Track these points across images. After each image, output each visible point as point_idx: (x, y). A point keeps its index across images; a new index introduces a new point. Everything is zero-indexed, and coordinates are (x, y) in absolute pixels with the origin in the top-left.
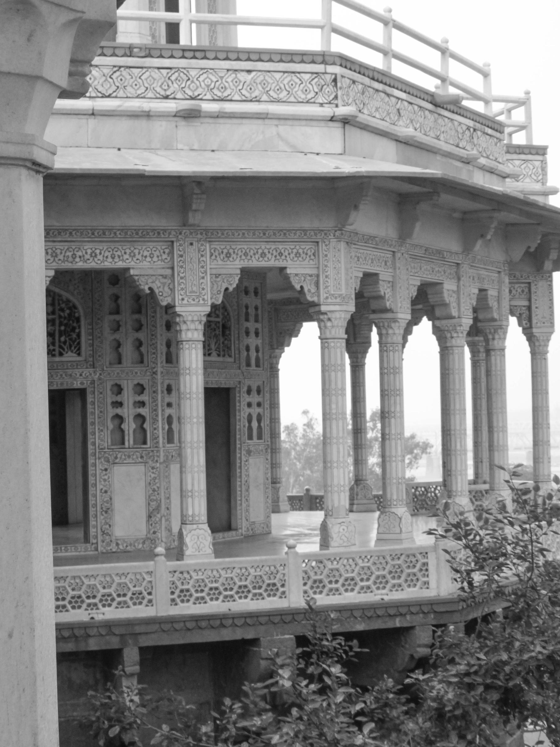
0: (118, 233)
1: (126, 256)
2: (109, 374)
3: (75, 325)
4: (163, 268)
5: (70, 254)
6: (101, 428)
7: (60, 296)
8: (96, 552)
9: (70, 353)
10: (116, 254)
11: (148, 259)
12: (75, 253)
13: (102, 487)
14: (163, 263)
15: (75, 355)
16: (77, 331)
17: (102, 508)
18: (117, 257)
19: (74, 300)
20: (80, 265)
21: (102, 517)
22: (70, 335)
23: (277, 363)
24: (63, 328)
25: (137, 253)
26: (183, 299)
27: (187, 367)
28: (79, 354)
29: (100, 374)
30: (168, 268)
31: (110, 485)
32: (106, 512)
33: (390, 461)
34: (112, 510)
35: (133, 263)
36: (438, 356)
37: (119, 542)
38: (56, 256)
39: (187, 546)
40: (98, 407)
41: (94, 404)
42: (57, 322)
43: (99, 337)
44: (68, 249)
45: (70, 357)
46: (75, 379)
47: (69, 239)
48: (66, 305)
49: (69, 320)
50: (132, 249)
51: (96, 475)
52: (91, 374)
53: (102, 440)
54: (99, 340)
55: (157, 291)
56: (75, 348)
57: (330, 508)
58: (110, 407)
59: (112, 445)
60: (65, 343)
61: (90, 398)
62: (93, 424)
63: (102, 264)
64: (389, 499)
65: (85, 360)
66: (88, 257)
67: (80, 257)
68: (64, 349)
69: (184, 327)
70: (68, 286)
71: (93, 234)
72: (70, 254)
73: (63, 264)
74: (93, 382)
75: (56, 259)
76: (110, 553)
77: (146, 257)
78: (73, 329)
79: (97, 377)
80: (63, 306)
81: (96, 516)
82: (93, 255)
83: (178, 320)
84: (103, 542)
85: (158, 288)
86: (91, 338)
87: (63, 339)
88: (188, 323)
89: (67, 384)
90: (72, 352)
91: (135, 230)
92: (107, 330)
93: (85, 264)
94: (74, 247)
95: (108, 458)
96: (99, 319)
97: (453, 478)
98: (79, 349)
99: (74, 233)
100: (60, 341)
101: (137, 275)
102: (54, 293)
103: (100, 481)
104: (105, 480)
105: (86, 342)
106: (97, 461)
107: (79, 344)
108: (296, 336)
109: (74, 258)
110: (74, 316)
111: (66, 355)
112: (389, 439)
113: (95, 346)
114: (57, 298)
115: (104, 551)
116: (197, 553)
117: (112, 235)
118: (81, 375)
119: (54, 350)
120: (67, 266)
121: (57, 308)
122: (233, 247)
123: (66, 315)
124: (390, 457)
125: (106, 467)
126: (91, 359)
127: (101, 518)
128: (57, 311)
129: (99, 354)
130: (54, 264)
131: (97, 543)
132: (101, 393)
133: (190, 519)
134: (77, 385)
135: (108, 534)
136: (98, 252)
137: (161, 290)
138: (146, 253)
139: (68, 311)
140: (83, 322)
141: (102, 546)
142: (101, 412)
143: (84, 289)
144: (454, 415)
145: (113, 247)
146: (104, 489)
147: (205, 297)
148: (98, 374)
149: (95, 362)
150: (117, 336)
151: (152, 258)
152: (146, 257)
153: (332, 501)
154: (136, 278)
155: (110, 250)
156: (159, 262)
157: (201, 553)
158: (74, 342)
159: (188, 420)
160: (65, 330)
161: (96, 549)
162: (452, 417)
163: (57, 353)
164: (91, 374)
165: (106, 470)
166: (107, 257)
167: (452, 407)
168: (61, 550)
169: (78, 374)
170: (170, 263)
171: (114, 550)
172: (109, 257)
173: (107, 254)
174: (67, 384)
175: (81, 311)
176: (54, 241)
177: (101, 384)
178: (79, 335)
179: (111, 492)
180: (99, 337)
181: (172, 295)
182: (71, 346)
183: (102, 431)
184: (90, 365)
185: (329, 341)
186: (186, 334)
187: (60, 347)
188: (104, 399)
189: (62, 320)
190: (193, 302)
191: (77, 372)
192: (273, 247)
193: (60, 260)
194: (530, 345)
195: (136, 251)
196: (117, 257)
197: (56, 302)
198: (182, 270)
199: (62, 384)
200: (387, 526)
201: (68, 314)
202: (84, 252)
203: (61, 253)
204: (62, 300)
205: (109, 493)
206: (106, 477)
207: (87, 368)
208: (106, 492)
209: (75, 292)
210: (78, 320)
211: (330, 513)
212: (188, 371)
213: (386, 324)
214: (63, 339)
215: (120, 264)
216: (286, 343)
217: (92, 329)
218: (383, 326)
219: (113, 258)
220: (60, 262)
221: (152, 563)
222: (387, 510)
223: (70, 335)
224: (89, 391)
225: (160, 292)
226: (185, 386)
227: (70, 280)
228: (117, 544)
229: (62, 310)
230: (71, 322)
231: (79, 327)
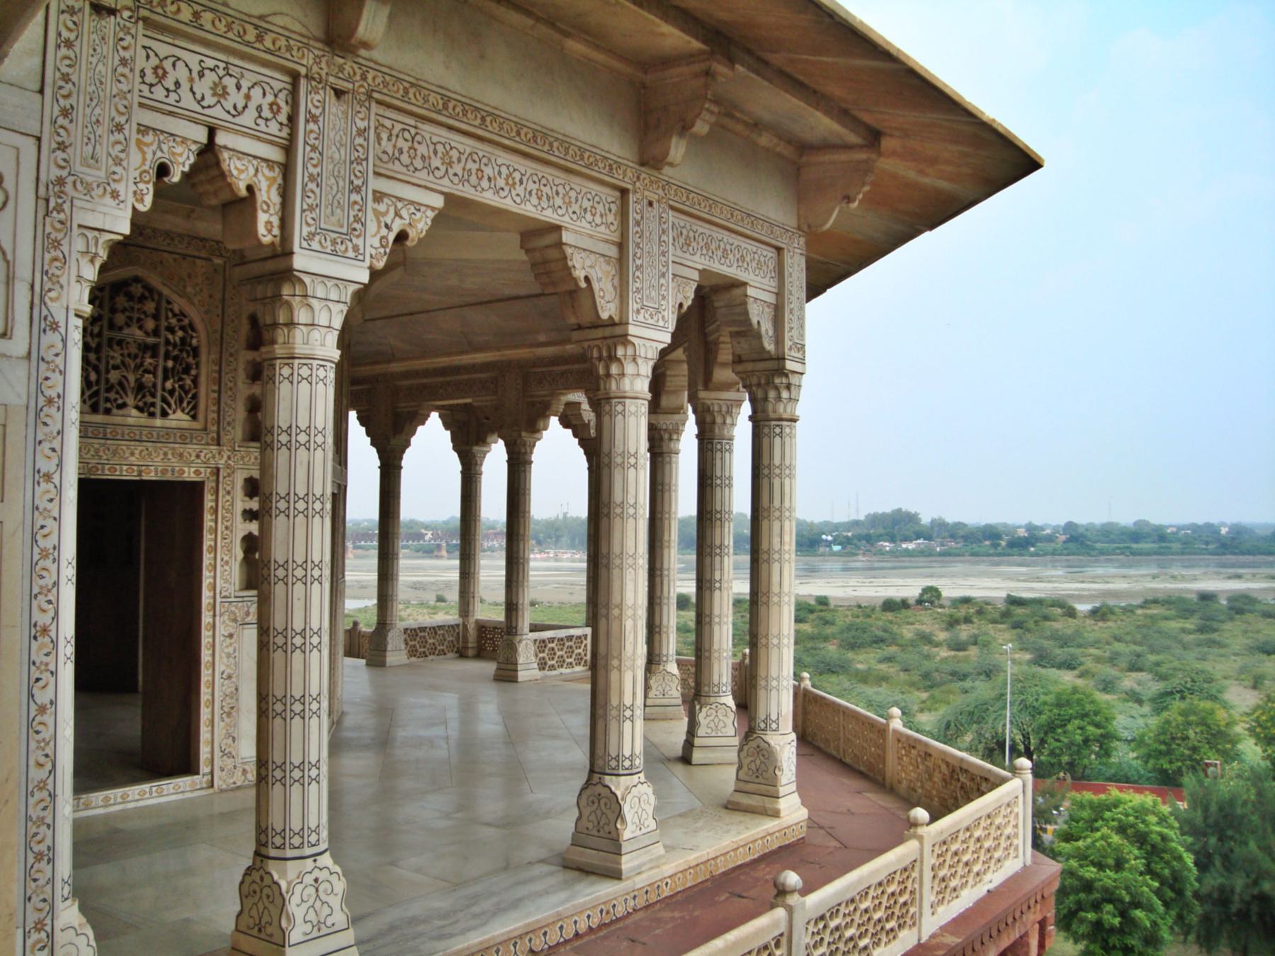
0: (556, 144)
1: (558, 201)
2: (243, 458)
3: (190, 360)
4: (607, 241)
5: (474, 167)
6: (226, 558)
7: (169, 303)
8: (211, 791)
9: (179, 411)
10: (546, 190)
11: (589, 217)
12: (483, 167)
13: (223, 668)
14: (607, 231)
15: (187, 417)
16: (193, 372)
17: (222, 708)
18: (544, 198)
19: (194, 315)
20: (489, 198)
21: (222, 724)
22: (181, 379)
23: (401, 458)
24: (170, 364)
25: (573, 200)
26: (638, 312)
27: (632, 452)
28: (194, 417)
29: (229, 458)
30: (613, 243)
31: (236, 665)
32: (229, 714)
33: (719, 624)
34: (238, 711)
35: (566, 218)
36: (505, 466)
37: (247, 767)
38: (450, 164)
39: (624, 821)
40: (223, 518)
41: (216, 511)
42: (162, 351)
43: (231, 389)
44: (470, 154)
45: (178, 418)
46: (189, 464)
47: (480, 132)
48: (179, 320)
49: (181, 351)
50: (568, 188)
51: (214, 646)
52: (214, 457)
53: (226, 581)
54: (230, 393)
55: (596, 286)
56: (189, 403)
57: (774, 717)
58: (239, 518)
59: (241, 590)
60: (172, 392)
61: (208, 502)
62: (214, 549)
63: (523, 206)
64: (716, 682)
65: (205, 429)
66: (501, 182)
67: (489, 179)
68: (169, 405)
69: (629, 368)
70: (185, 287)
71: (518, 134)
72: (474, 167)
73: (460, 186)
74: (217, 471)
75: (451, 172)
76: (232, 790)
77: (585, 210)
78: (187, 370)
79: (223, 462)
80: (174, 321)
81: (212, 721)
82: (510, 182)
83: (620, 352)
84: (222, 770)
85: (600, 280)
86: (216, 388)
87: (169, 385)
88: (640, 361)
89: (173, 471)
90: (183, 411)
91: (580, 148)
92: (241, 375)
93: (496, 198)
94: (481, 154)
95: (233, 613)
96: (231, 355)
97: (664, 636)
98: (195, 408)
99: (489, 119)
100: (164, 389)
101: (571, 246)
102: (160, 295)
103: (221, 657)
104: (229, 656)
105: (207, 394)
106: (217, 618)
107: (195, 397)
108: (423, 424)
109: (480, 179)
110: (190, 345)
111: (171, 417)
112: (720, 589)
113: (223, 405)
114: (164, 304)
115: (224, 787)
116: (638, 833)
117: (546, 148)
118: (198, 456)
119: (153, 405)
120: (467, 192)
121: (164, 324)
122: (695, 228)
123: (177, 339)
124: (720, 616)
125: (232, 631)
126: (215, 428)
127: (220, 727)
128: (163, 332)
129: (228, 419)
130: (446, 181)
131: (212, 773)
132: (228, 493)
133: (627, 764)
134: (189, 475)
135: (230, 755)
136: (517, 176)
137: (602, 285)
138: (586, 204)
139: (180, 333)
140: (203, 357)
141: (220, 778)
142: (227, 528)
143: (211, 296)
144: (669, 547)
145: (540, 175)
146: (228, 671)
147: (665, 313)
148: (225, 457)
149: (222, 433)
150: (256, 389)
151: (594, 215)
152: (585, 210)
153: (779, 704)
154: (569, 251)
155: (535, 178)
156: (602, 229)
157: (644, 830)
158: (187, 393)
159: (630, 561)
160: (174, 368)
161: (212, 786)
162: (666, 552)
163: (158, 411)
164: (214, 457)
165: (231, 636)
166: (530, 192)
167: (666, 538)
168: (151, 793)
169: (194, 454)
170: (617, 234)
171: (239, 784)
172: (534, 192)
173: (531, 186)
174: (173, 471)
175: (200, 339)
176: (450, 128)
177: (229, 475)
178: (195, 381)
179: (238, 677)
180: (231, 389)
181: (617, 301)
182: (181, 401)
183: (227, 563)
184: (212, 439)
185: (785, 423)
186: (632, 383)
187: (164, 400)
188: (232, 505)
189: (170, 348)
190: (650, 321)
191: (192, 449)
192: (736, 243)
193: (455, 175)
194: (588, 460)
195: (573, 194)
196: (544, 198)
197: (163, 312)
198: (639, 251)
199: (164, 472)
200: (712, 724)
201: (183, 340)
202: (497, 169)
203: (459, 160)
204: (172, 310)
205: (234, 679)
206: (230, 650)
207: (208, 444)
208: (229, 677)
209: (196, 301)
210: (195, 352)
211: (774, 726)
212: (632, 461)
213: (724, 409)
214: (169, 385)
215: (549, 216)
216: (541, 424)
217: (220, 372)
218: (720, 411)
219: (539, 198)
220: (456, 180)
221: (780, 913)
222: (712, 699)
223: (181, 379)
224: (209, 486)
225: (601, 290)
226: (625, 490)
227: (189, 276)
228: (244, 772)
229: (171, 329)
230: (185, 355)
231: (197, 365)
